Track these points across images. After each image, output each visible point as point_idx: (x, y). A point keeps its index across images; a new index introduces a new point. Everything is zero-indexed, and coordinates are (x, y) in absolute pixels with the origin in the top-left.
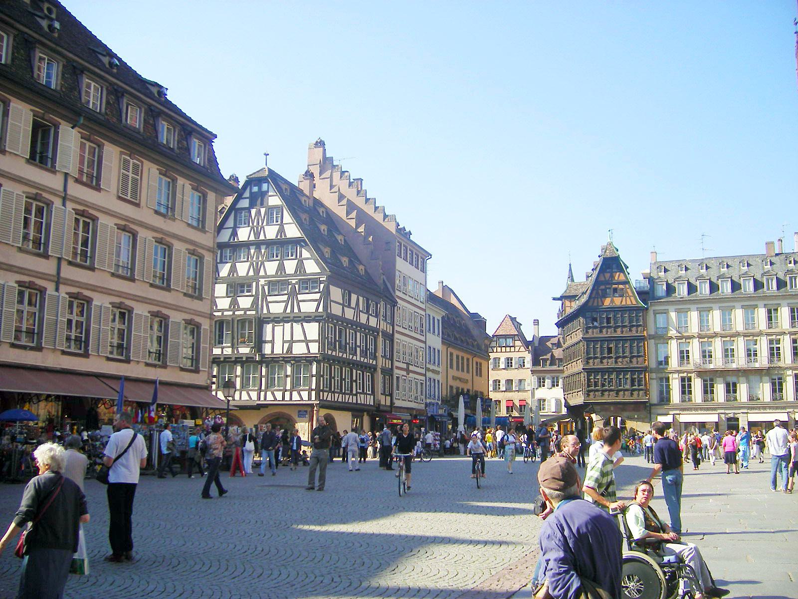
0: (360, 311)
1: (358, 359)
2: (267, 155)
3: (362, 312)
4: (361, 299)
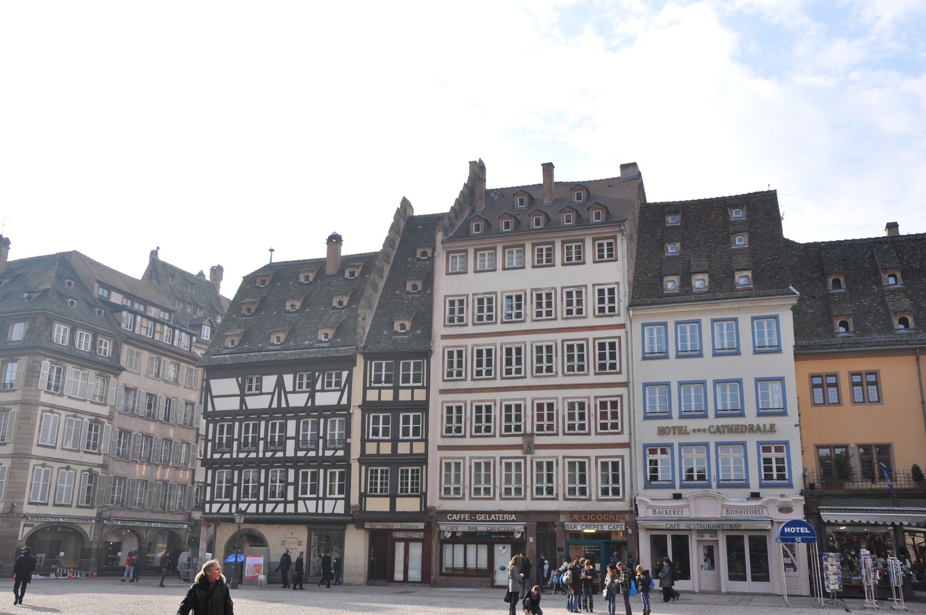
0: (286, 393)
1: (290, 453)
2: (272, 250)
3: (294, 392)
4: (288, 379)
